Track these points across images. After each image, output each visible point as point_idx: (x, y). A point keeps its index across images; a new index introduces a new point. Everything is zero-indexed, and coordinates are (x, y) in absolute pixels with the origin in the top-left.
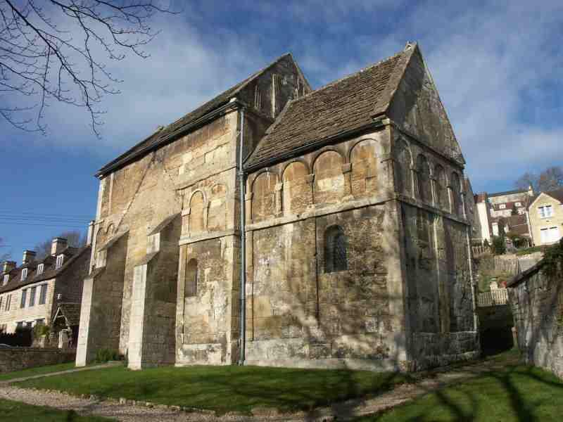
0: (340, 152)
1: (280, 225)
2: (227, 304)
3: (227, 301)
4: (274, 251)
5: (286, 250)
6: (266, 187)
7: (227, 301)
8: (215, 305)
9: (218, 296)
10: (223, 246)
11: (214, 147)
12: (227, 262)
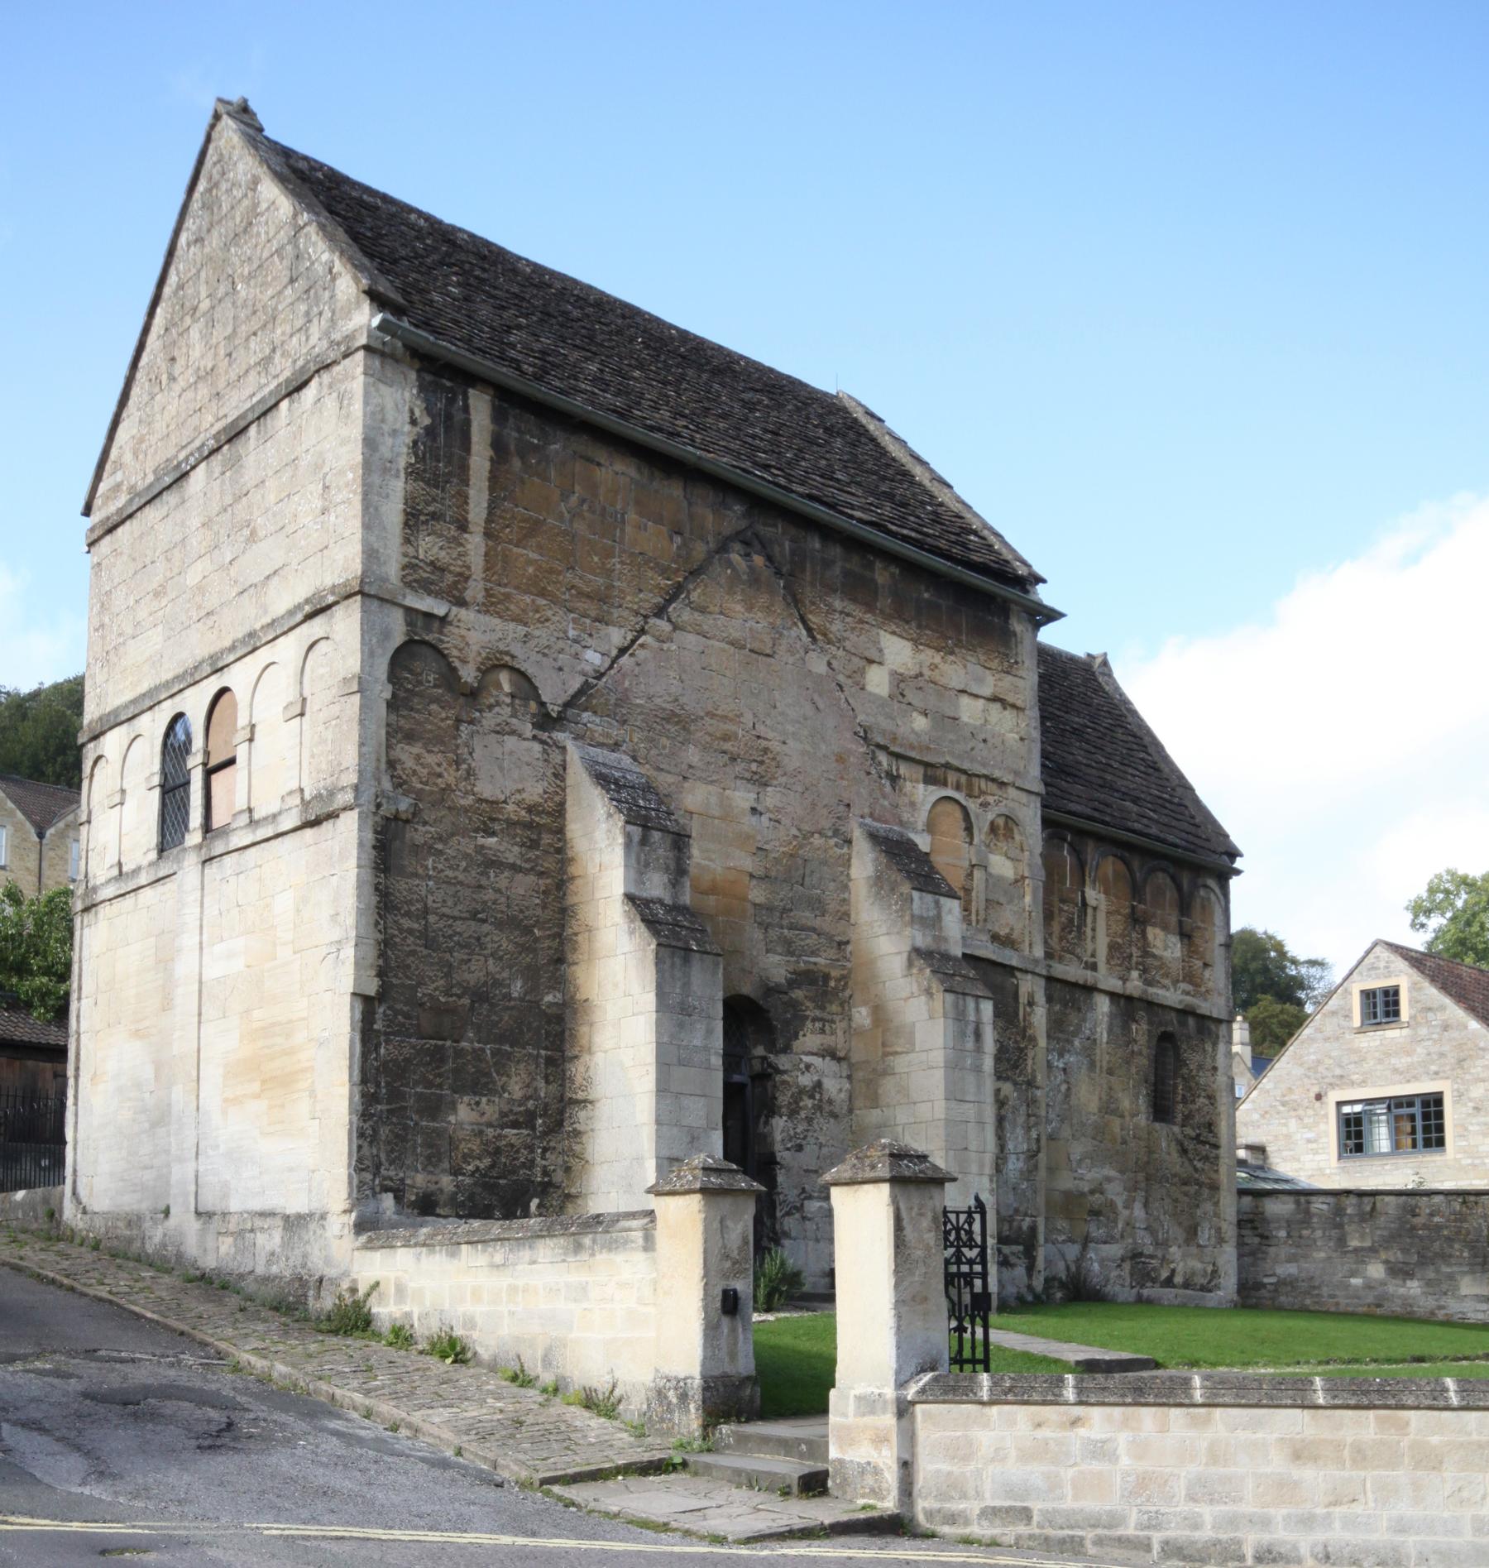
0: (1179, 888)
1: (1090, 989)
2: (1038, 1151)
3: (1038, 1140)
4: (1077, 1043)
5: (1098, 1051)
6: (1062, 881)
7: (1038, 1140)
8: (1010, 1146)
9: (1015, 1126)
10: (1023, 999)
11: (987, 691)
12: (1033, 1040)
